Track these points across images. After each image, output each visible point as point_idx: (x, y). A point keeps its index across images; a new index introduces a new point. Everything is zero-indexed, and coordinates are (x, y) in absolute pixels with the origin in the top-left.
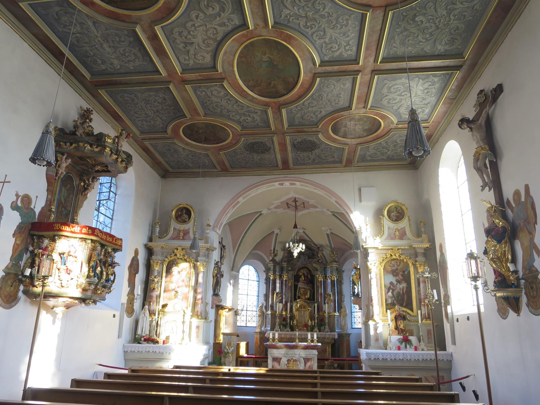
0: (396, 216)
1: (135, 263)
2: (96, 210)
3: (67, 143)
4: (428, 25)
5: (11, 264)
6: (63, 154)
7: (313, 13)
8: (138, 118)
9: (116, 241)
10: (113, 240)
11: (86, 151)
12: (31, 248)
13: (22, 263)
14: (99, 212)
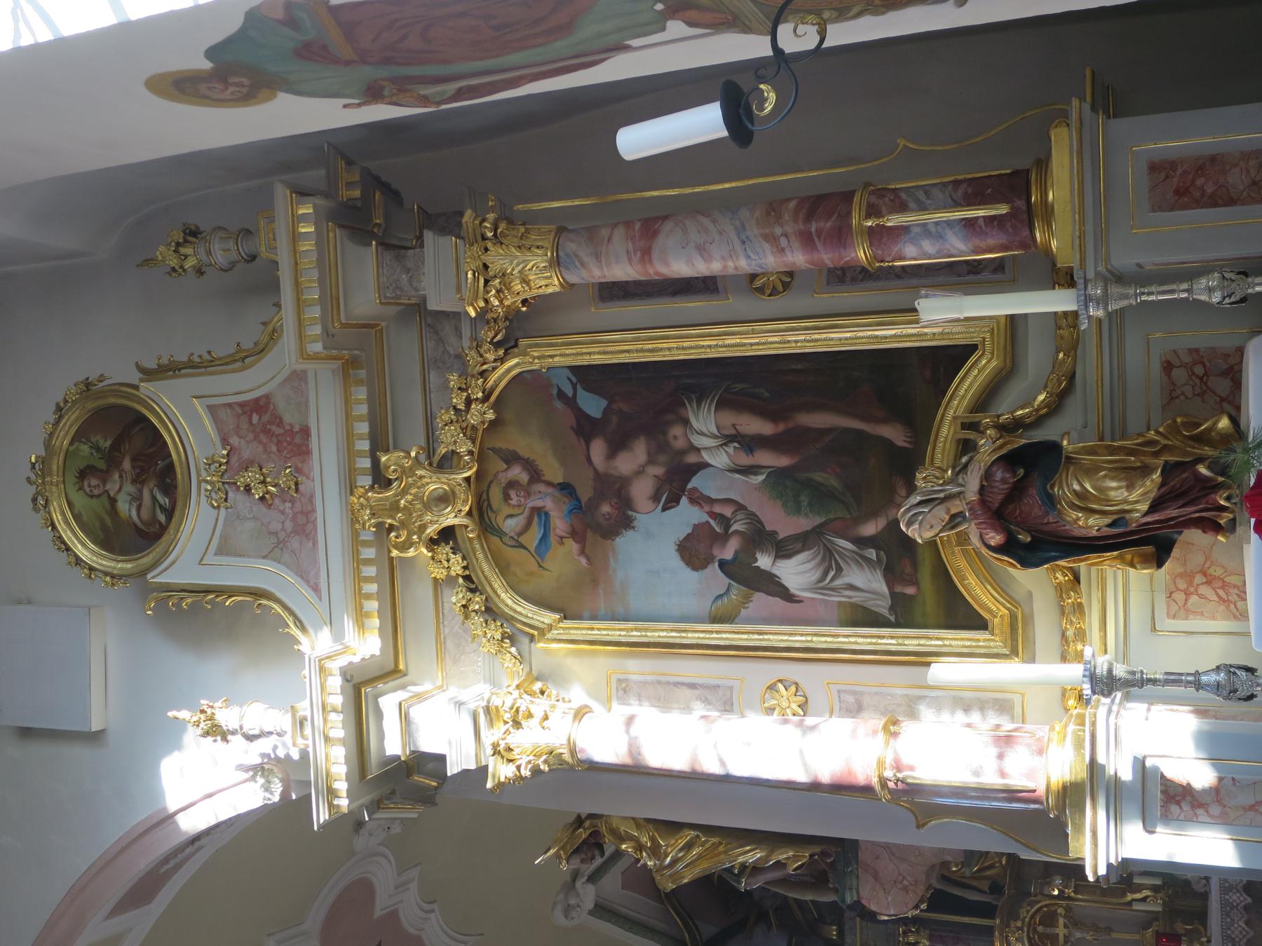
0: (138, 480)
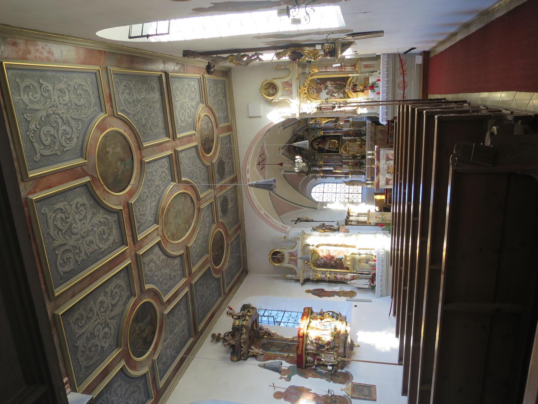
0: (272, 89)
1: (316, 292)
2: (280, 325)
3: (241, 350)
4: (146, 114)
5: (325, 378)
6: (249, 352)
8: (212, 301)
9: (306, 313)
10: (305, 315)
11: (246, 338)
12: (314, 367)
13: (324, 372)
14: (281, 322)
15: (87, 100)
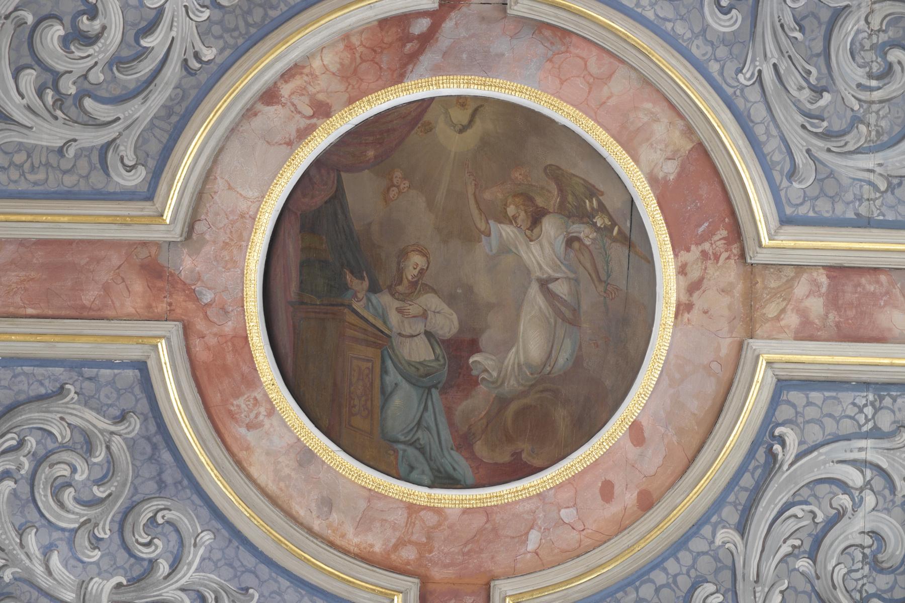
7: (119, 585)
15: (856, 121)
